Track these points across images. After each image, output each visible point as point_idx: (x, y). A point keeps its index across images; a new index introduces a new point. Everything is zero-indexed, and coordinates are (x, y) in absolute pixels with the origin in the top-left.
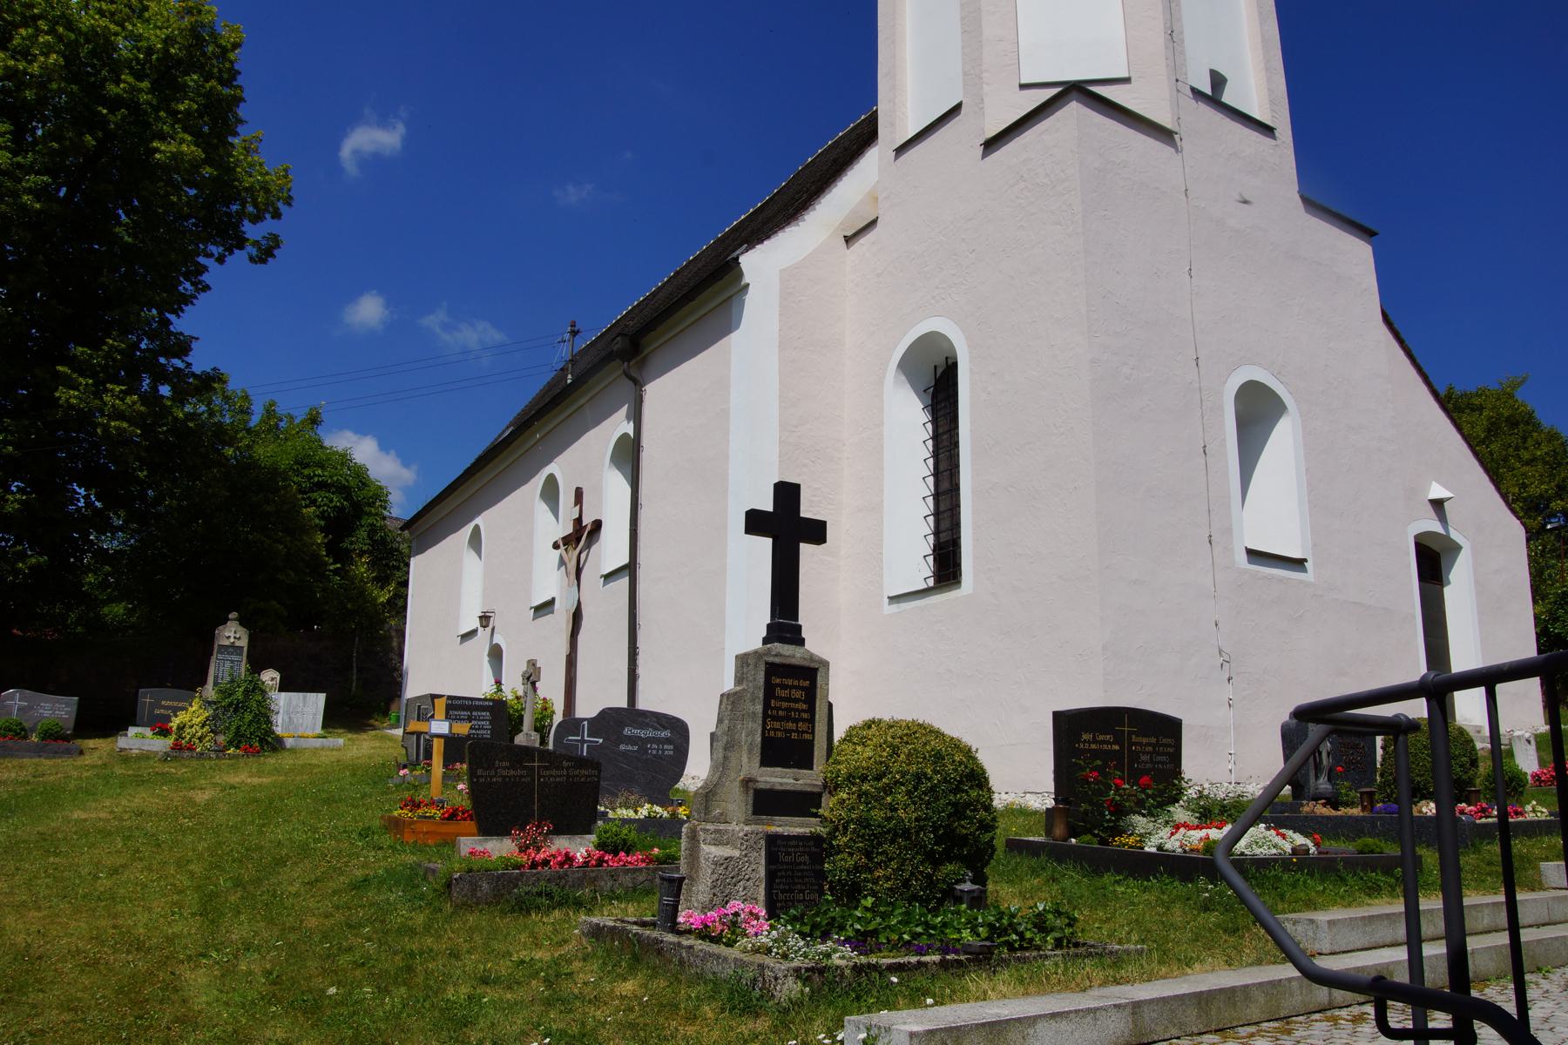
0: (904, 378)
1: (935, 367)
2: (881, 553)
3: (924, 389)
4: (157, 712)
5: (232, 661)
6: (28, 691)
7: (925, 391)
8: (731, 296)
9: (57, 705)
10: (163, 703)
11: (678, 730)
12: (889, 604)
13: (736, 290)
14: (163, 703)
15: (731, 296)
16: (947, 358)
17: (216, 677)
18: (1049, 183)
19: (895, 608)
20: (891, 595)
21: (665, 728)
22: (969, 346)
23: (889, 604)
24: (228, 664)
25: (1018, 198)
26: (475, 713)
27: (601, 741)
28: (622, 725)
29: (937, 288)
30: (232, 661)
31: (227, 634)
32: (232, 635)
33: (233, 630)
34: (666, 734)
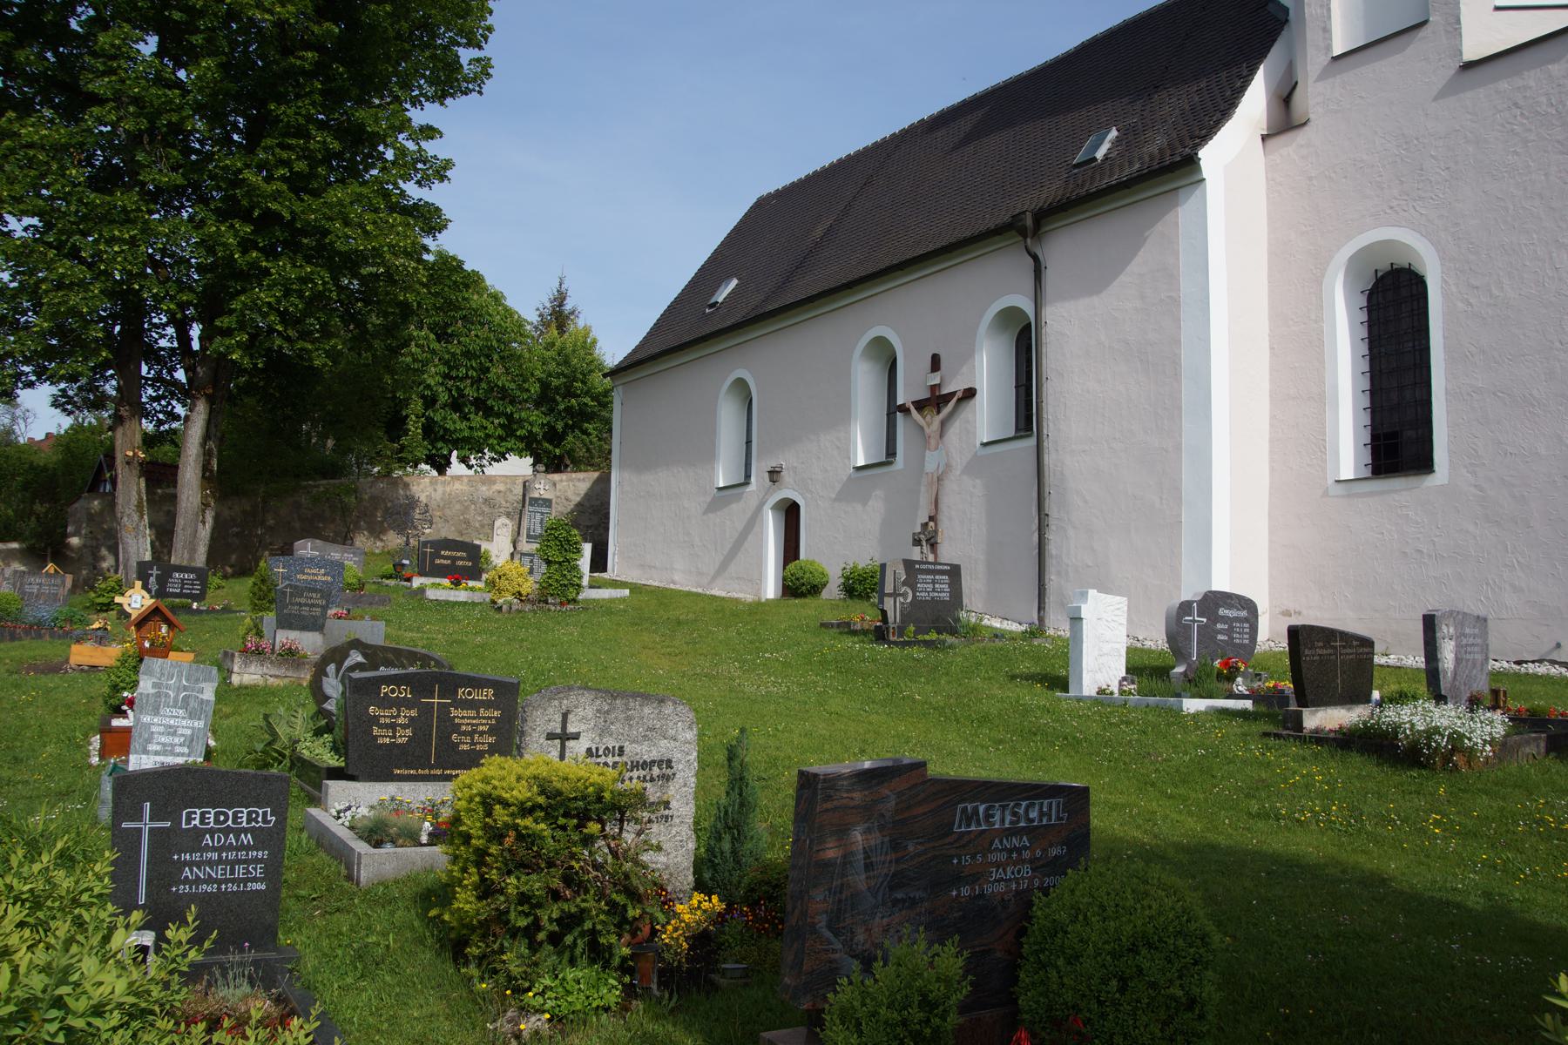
1: (1376, 271)
4: (438, 561)
5: (542, 514)
6: (318, 541)
8: (1178, 188)
9: (346, 555)
10: (443, 553)
11: (1249, 606)
13: (1189, 182)
14: (443, 553)
15: (1178, 188)
17: (529, 529)
21: (1244, 609)
24: (538, 516)
25: (1509, 123)
26: (937, 577)
27: (1205, 620)
28: (1218, 606)
29: (1396, 199)
30: (542, 514)
31: (537, 486)
32: (542, 486)
33: (543, 482)
34: (1244, 614)
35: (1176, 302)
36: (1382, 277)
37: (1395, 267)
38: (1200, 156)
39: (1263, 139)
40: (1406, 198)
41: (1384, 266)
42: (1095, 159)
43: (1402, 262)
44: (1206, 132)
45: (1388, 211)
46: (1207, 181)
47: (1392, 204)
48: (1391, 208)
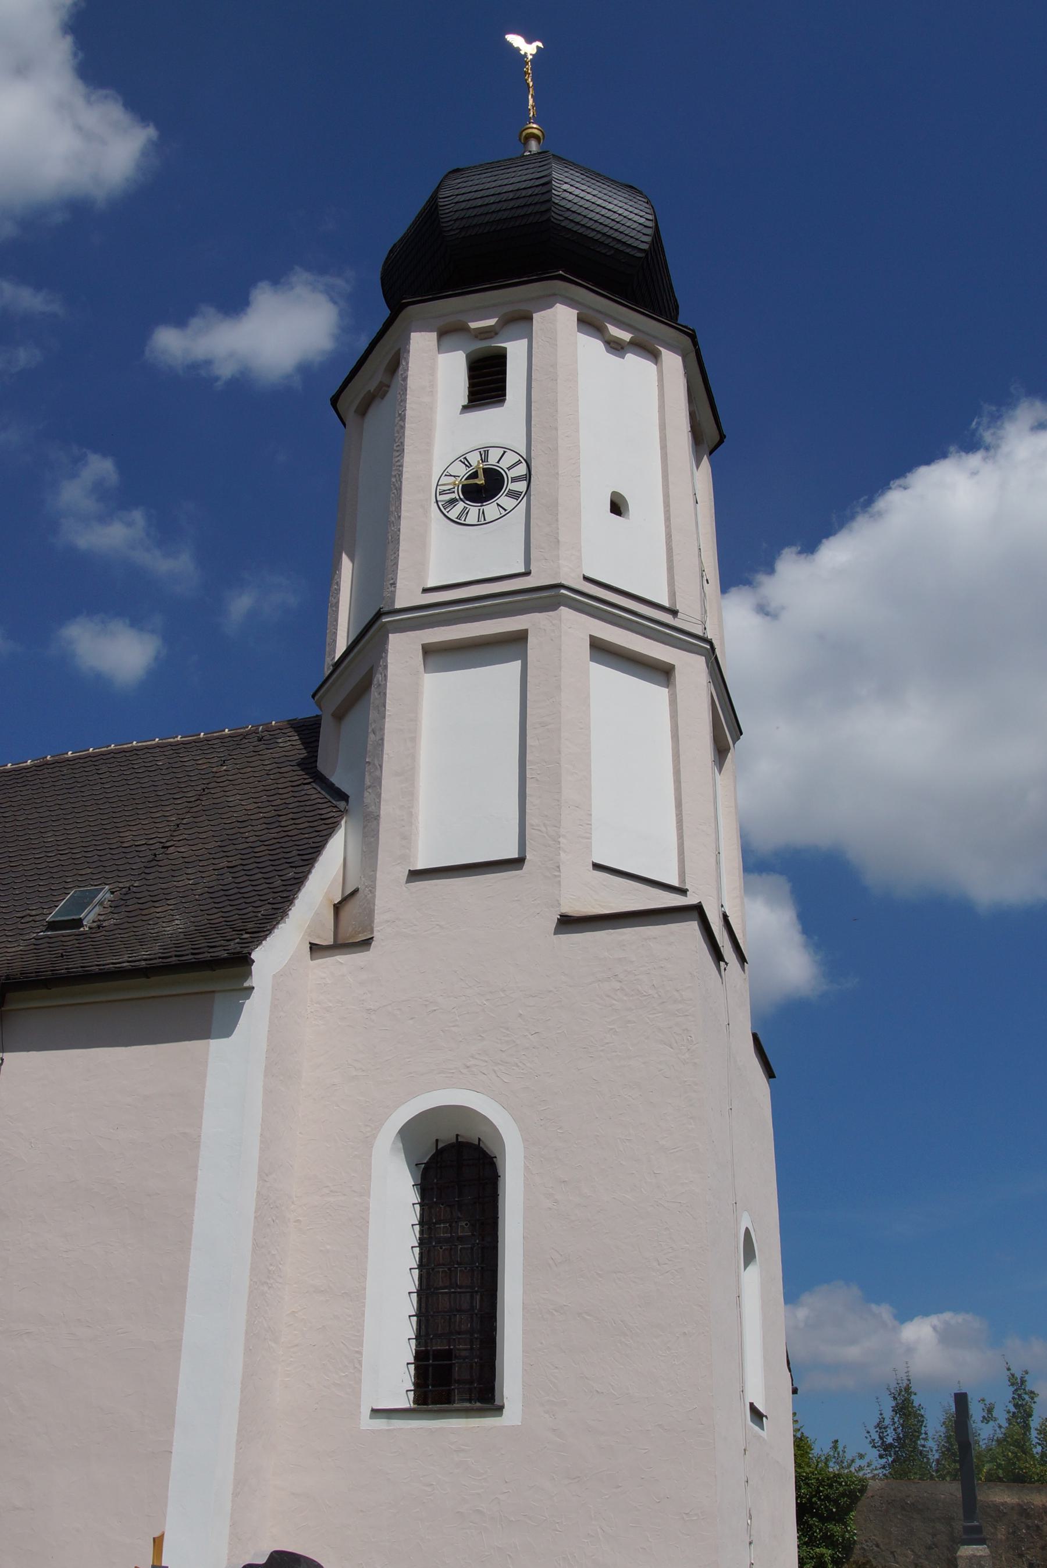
0: (401, 1145)
1: (437, 1141)
2: (360, 1353)
3: (416, 1163)
7: (416, 1165)
8: (213, 992)
12: (371, 1418)
15: (213, 992)
16: (457, 1135)
18: (656, 996)
19: (381, 1424)
20: (375, 1408)
22: (525, 1140)
23: (371, 1418)
25: (608, 996)
29: (472, 1057)
35: (195, 1143)
36: (444, 1149)
37: (460, 1139)
38: (253, 956)
39: (311, 948)
40: (487, 1059)
41: (447, 1136)
42: (79, 923)
43: (470, 1135)
44: (262, 930)
45: (464, 1071)
46: (255, 994)
47: (468, 1064)
48: (468, 1067)
